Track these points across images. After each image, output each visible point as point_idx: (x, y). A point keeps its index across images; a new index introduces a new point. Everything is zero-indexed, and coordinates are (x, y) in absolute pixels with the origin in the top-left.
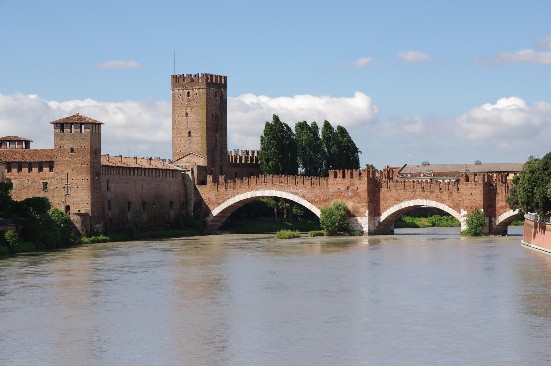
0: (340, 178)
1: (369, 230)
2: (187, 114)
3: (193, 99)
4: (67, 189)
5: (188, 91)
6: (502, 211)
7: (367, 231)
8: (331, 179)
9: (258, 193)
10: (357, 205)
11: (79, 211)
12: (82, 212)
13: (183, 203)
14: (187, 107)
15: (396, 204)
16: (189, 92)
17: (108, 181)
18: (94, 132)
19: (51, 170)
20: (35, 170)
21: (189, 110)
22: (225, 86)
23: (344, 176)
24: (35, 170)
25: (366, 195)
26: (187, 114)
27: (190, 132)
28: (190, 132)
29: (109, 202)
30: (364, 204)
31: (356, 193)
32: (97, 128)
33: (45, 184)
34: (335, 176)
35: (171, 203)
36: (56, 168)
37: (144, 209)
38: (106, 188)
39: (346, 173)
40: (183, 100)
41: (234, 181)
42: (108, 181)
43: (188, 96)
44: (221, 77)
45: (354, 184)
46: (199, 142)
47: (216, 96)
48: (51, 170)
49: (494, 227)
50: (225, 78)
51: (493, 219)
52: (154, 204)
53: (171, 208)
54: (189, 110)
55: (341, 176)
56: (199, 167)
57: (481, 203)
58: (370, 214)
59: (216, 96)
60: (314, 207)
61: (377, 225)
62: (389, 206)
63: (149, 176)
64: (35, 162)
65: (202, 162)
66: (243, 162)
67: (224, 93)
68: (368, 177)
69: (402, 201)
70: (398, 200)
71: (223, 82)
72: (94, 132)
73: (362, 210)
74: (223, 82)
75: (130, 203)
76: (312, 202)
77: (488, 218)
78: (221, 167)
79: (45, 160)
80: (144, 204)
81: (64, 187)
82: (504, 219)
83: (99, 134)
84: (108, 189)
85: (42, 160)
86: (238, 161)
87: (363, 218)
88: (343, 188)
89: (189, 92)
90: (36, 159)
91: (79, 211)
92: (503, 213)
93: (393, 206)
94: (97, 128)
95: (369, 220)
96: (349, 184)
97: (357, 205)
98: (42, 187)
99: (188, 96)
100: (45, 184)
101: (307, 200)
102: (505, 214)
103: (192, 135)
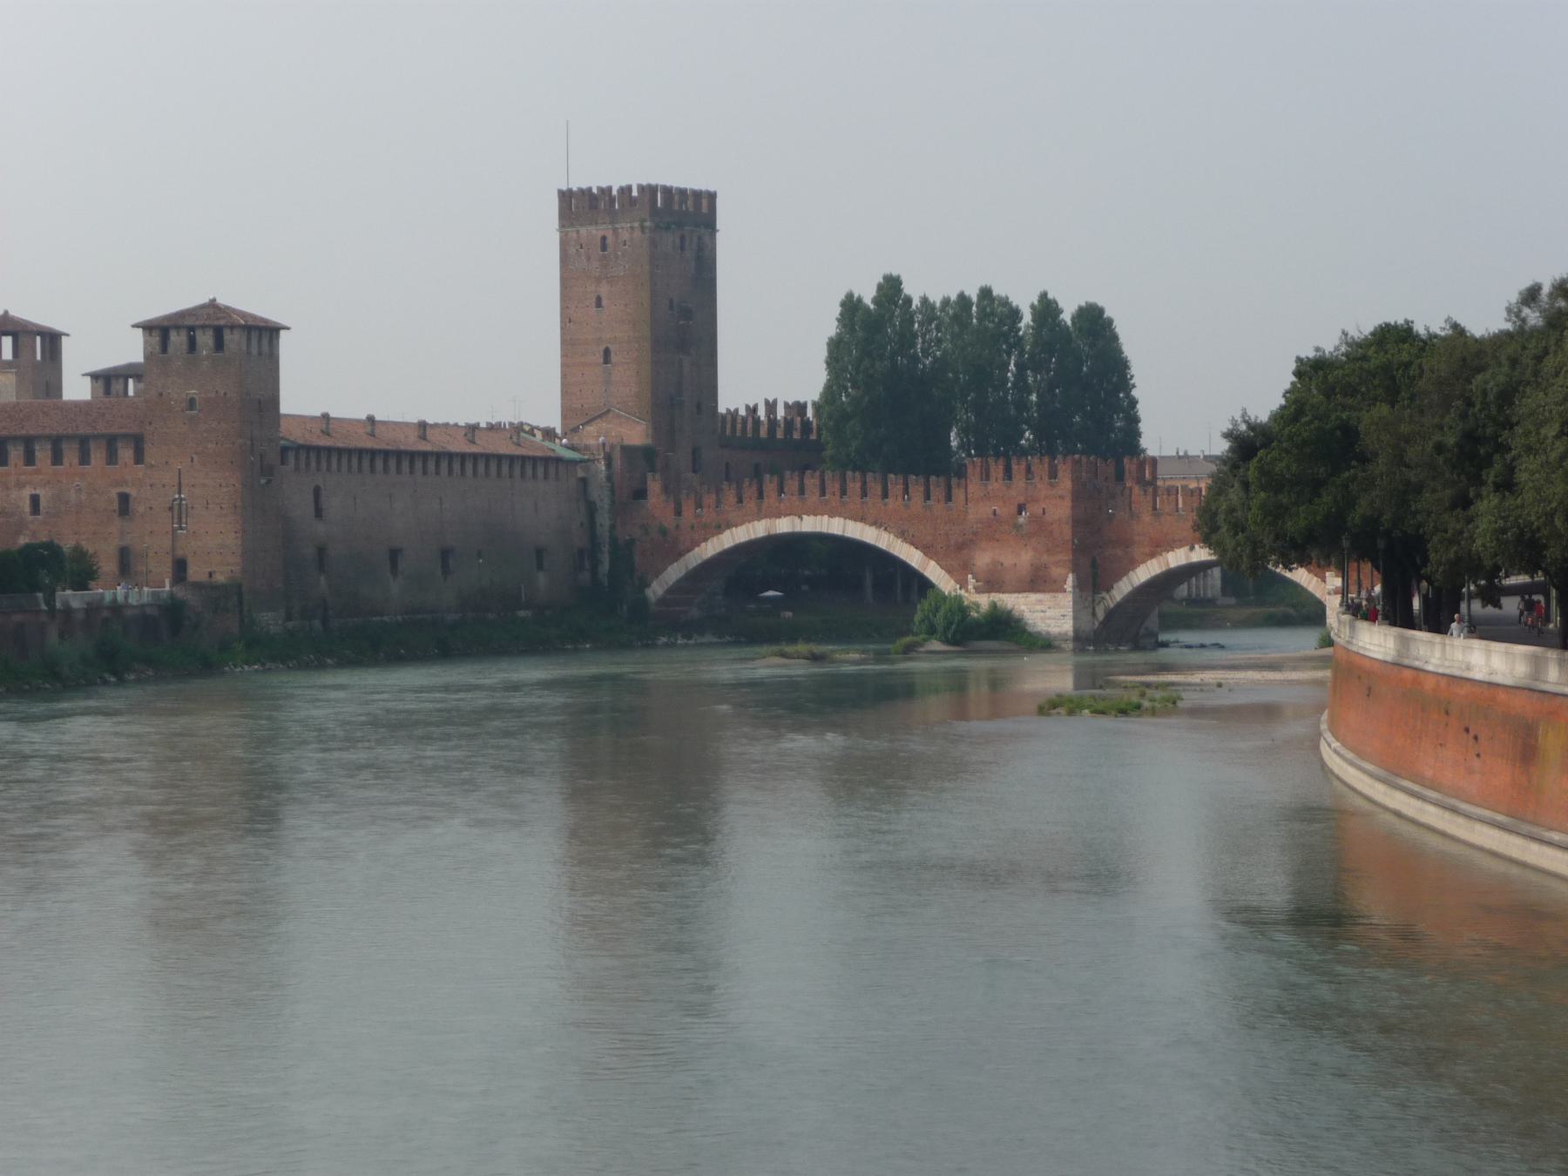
0: (996, 485)
1: (1076, 631)
2: (599, 300)
3: (617, 257)
4: (178, 512)
5: (600, 234)
7: (1071, 634)
8: (974, 486)
9: (784, 525)
10: (1045, 559)
11: (210, 575)
12: (220, 578)
14: (598, 280)
15: (1152, 555)
16: (604, 238)
17: (317, 492)
18: (254, 351)
19: (139, 458)
20: (98, 455)
21: (604, 290)
22: (707, 222)
23: (1008, 473)
24: (98, 455)
25: (1067, 532)
26: (599, 300)
27: (607, 352)
28: (607, 352)
29: (321, 551)
30: (1061, 557)
31: (1040, 526)
32: (265, 342)
33: (124, 499)
34: (986, 476)
35: (539, 553)
36: (151, 453)
37: (446, 570)
38: (311, 510)
39: (1015, 467)
40: (589, 259)
41: (719, 491)
42: (317, 492)
43: (604, 247)
44: (697, 195)
45: (1035, 500)
46: (628, 379)
47: (682, 248)
48: (139, 458)
50: (712, 197)
52: (480, 555)
53: (540, 567)
54: (604, 290)
55: (1001, 475)
56: (628, 451)
58: (1080, 586)
59: (682, 248)
60: (933, 563)
61: (1101, 615)
62: (1133, 564)
63: (437, 473)
64: (96, 437)
65: (636, 434)
66: (780, 435)
68: (1076, 481)
69: (1171, 545)
70: (1159, 546)
71: (705, 210)
72: (254, 351)
73: (1056, 572)
74: (705, 210)
75: (394, 554)
76: (928, 550)
78: (695, 453)
79: (123, 431)
80: (445, 554)
81: (171, 509)
83: (272, 358)
84: (319, 513)
85: (114, 430)
86: (763, 433)
87: (1060, 595)
88: (1004, 511)
89: (604, 238)
90: (102, 429)
91: (210, 575)
93: (1144, 562)
94: (265, 342)
95: (1075, 603)
96: (1021, 500)
97: (1045, 559)
98: (116, 505)
99: (604, 247)
100: (124, 499)
101: (912, 544)
103: (614, 358)
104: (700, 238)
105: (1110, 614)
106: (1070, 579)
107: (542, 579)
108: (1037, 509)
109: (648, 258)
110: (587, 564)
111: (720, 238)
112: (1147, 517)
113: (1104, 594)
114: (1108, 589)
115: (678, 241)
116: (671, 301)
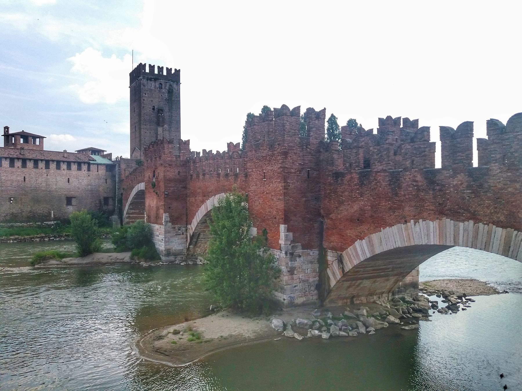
6: (350, 233)
13: (106, 199)
15: (203, 202)
49: (333, 283)
50: (178, 72)
51: (331, 257)
57: (281, 205)
58: (174, 220)
62: (199, 207)
67: (175, 86)
77: (314, 253)
82: (356, 262)
87: (162, 226)
92: (353, 242)
95: (166, 232)
102: (357, 243)
104: (170, 85)
105: (192, 238)
106: (165, 217)
107: (70, 208)
108: (156, 174)
109: (155, 94)
110: (111, 202)
111: (182, 86)
112: (201, 177)
113: (189, 226)
114: (188, 222)
115: (158, 86)
116: (154, 106)
